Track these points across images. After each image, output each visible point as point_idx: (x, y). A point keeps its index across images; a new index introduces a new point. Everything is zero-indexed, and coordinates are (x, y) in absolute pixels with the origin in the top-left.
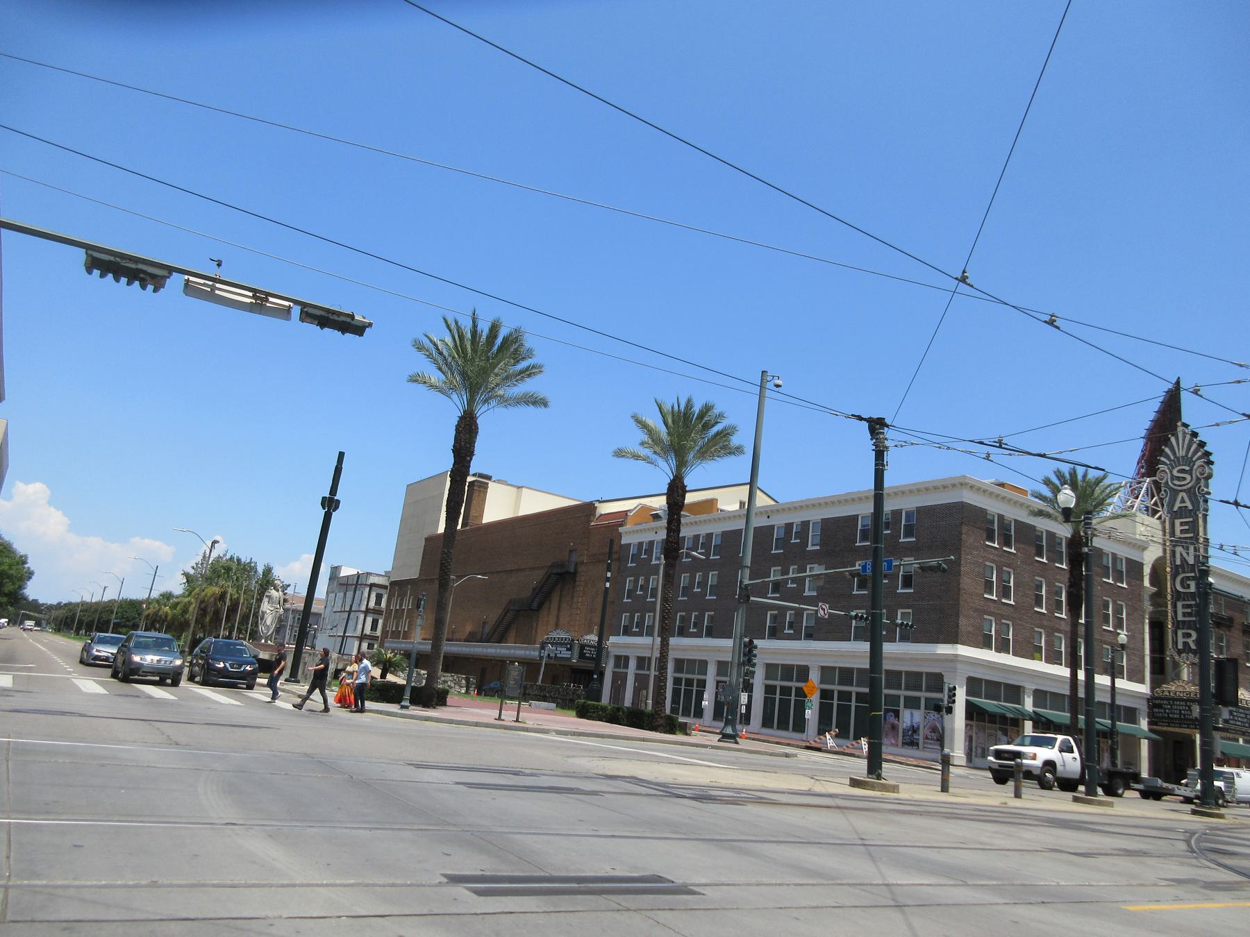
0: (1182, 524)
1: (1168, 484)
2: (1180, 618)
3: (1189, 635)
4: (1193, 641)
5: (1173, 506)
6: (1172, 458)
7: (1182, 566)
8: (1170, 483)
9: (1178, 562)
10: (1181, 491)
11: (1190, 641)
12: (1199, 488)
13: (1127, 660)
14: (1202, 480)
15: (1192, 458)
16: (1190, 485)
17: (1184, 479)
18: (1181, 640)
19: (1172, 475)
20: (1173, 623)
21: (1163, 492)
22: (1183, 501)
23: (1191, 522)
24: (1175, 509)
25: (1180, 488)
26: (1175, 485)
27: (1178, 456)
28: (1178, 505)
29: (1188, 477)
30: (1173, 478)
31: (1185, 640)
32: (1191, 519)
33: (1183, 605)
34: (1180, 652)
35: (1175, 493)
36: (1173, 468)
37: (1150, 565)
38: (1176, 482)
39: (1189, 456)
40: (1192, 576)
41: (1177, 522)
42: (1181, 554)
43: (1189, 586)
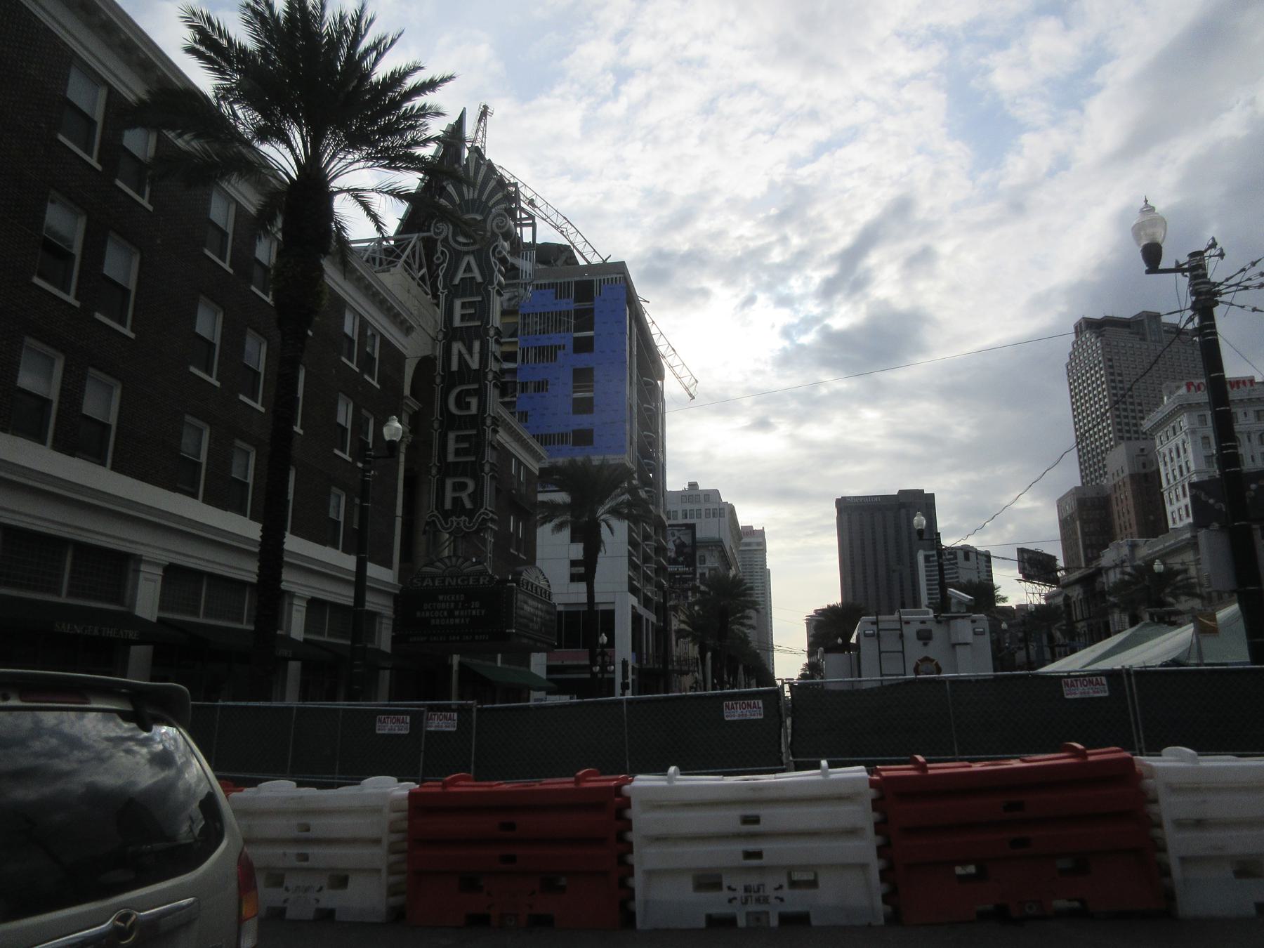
0: (464, 306)
1: (448, 243)
2: (451, 458)
3: (461, 487)
4: (469, 495)
6: (458, 201)
9: (454, 367)
11: (464, 496)
12: (494, 251)
14: (500, 237)
21: (439, 254)
22: (468, 268)
23: (479, 301)
24: (457, 281)
25: (466, 249)
26: (459, 243)
27: (466, 198)
28: (460, 275)
31: (457, 495)
32: (480, 299)
33: (457, 437)
35: (457, 256)
37: (416, 361)
38: (461, 239)
39: (484, 199)
40: (474, 389)
41: (458, 304)
42: (460, 354)
43: (468, 406)
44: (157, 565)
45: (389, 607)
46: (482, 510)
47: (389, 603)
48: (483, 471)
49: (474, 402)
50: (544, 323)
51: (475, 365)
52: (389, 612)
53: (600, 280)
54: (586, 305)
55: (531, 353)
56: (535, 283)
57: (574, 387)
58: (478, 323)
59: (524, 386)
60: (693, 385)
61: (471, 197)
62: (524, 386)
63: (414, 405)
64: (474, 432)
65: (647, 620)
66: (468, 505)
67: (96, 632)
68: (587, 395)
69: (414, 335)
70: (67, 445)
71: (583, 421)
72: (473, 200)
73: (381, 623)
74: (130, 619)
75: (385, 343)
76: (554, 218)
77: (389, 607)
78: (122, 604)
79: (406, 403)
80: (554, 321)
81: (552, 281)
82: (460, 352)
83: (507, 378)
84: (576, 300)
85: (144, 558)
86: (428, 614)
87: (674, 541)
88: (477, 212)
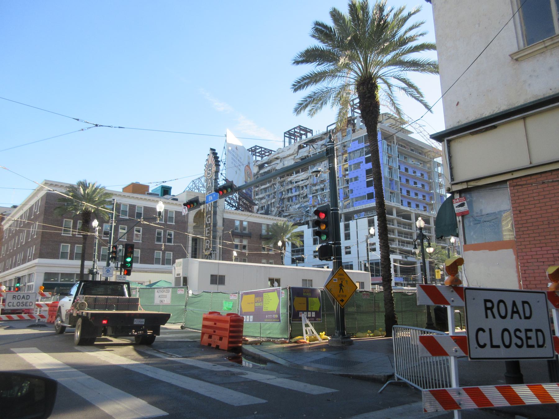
38: (209, 176)
51: (210, 210)
56: (352, 139)
57: (367, 177)
66: (209, 247)
81: (357, 137)
83: (347, 178)
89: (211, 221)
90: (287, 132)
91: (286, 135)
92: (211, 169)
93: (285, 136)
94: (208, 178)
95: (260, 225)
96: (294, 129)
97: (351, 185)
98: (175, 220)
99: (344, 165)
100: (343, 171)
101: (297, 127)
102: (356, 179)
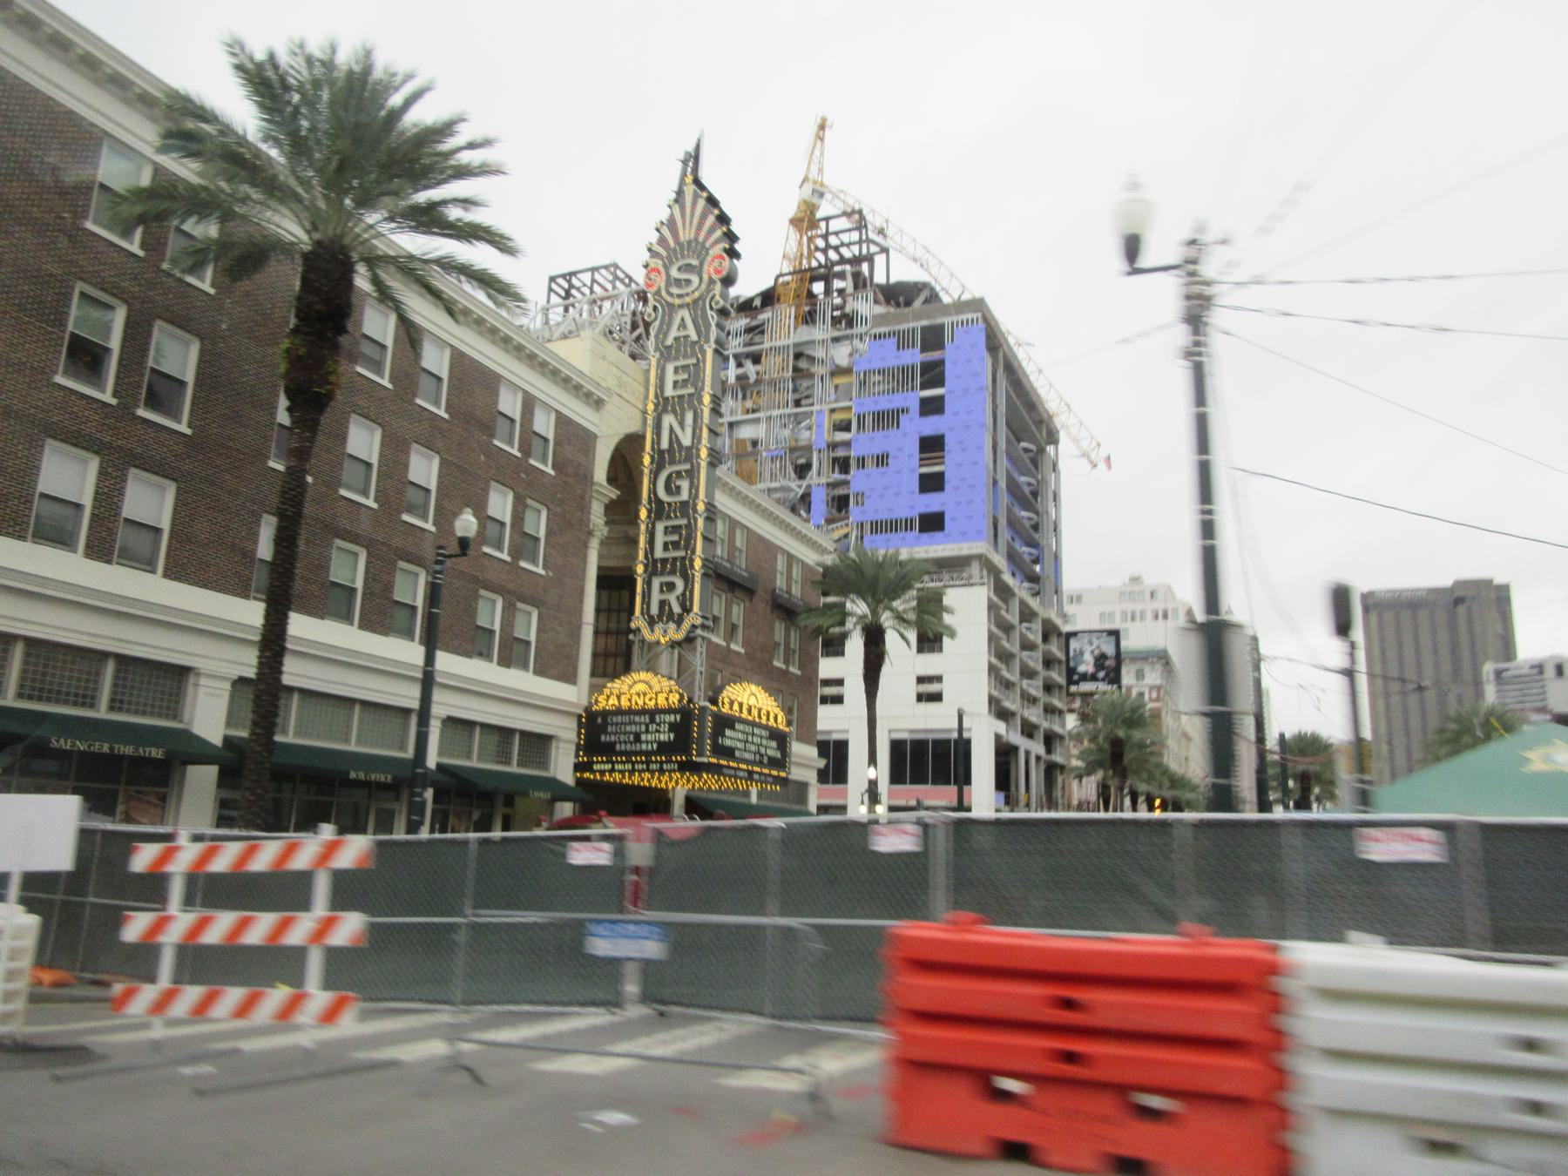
0: (676, 370)
2: (659, 553)
5: (666, 335)
7: (671, 450)
8: (664, 293)
9: (665, 445)
10: (681, 306)
13: (539, 631)
15: (704, 242)
16: (697, 294)
17: (688, 282)
18: (656, 597)
19: (668, 276)
20: (646, 566)
22: (683, 325)
24: (669, 341)
26: (671, 295)
28: (674, 333)
29: (695, 279)
30: (670, 282)
31: (664, 597)
32: (694, 361)
33: (666, 528)
34: (652, 622)
36: (671, 263)
38: (675, 291)
39: (701, 239)
40: (686, 471)
41: (670, 368)
42: (671, 429)
44: (225, 679)
45: (571, 729)
46: (691, 615)
47: (573, 724)
48: (692, 567)
49: (685, 485)
50: (888, 383)
52: (571, 735)
53: (953, 323)
54: (934, 355)
55: (869, 421)
56: (873, 332)
57: (921, 460)
58: (692, 390)
59: (861, 462)
60: (1094, 449)
61: (687, 238)
62: (861, 462)
63: (613, 493)
64: (683, 522)
65: (1027, 753)
66: (677, 609)
67: (106, 748)
68: (936, 469)
69: (608, 407)
70: (100, 549)
71: (932, 503)
72: (689, 242)
73: (557, 748)
74: (187, 735)
75: (563, 422)
76: (911, 249)
77: (571, 729)
78: (181, 722)
79: (597, 491)
80: (901, 377)
82: (683, 428)
83: (840, 453)
84: (924, 349)
85: (202, 671)
86: (613, 738)
87: (1092, 652)
88: (688, 256)
89: (694, 496)
90: (563, 276)
91: (554, 286)
92: (695, 262)
93: (550, 290)
94: (669, 299)
95: (771, 549)
96: (594, 270)
97: (858, 480)
98: (554, 451)
99: (833, 411)
100: (829, 432)
101: (606, 267)
102: (882, 460)
